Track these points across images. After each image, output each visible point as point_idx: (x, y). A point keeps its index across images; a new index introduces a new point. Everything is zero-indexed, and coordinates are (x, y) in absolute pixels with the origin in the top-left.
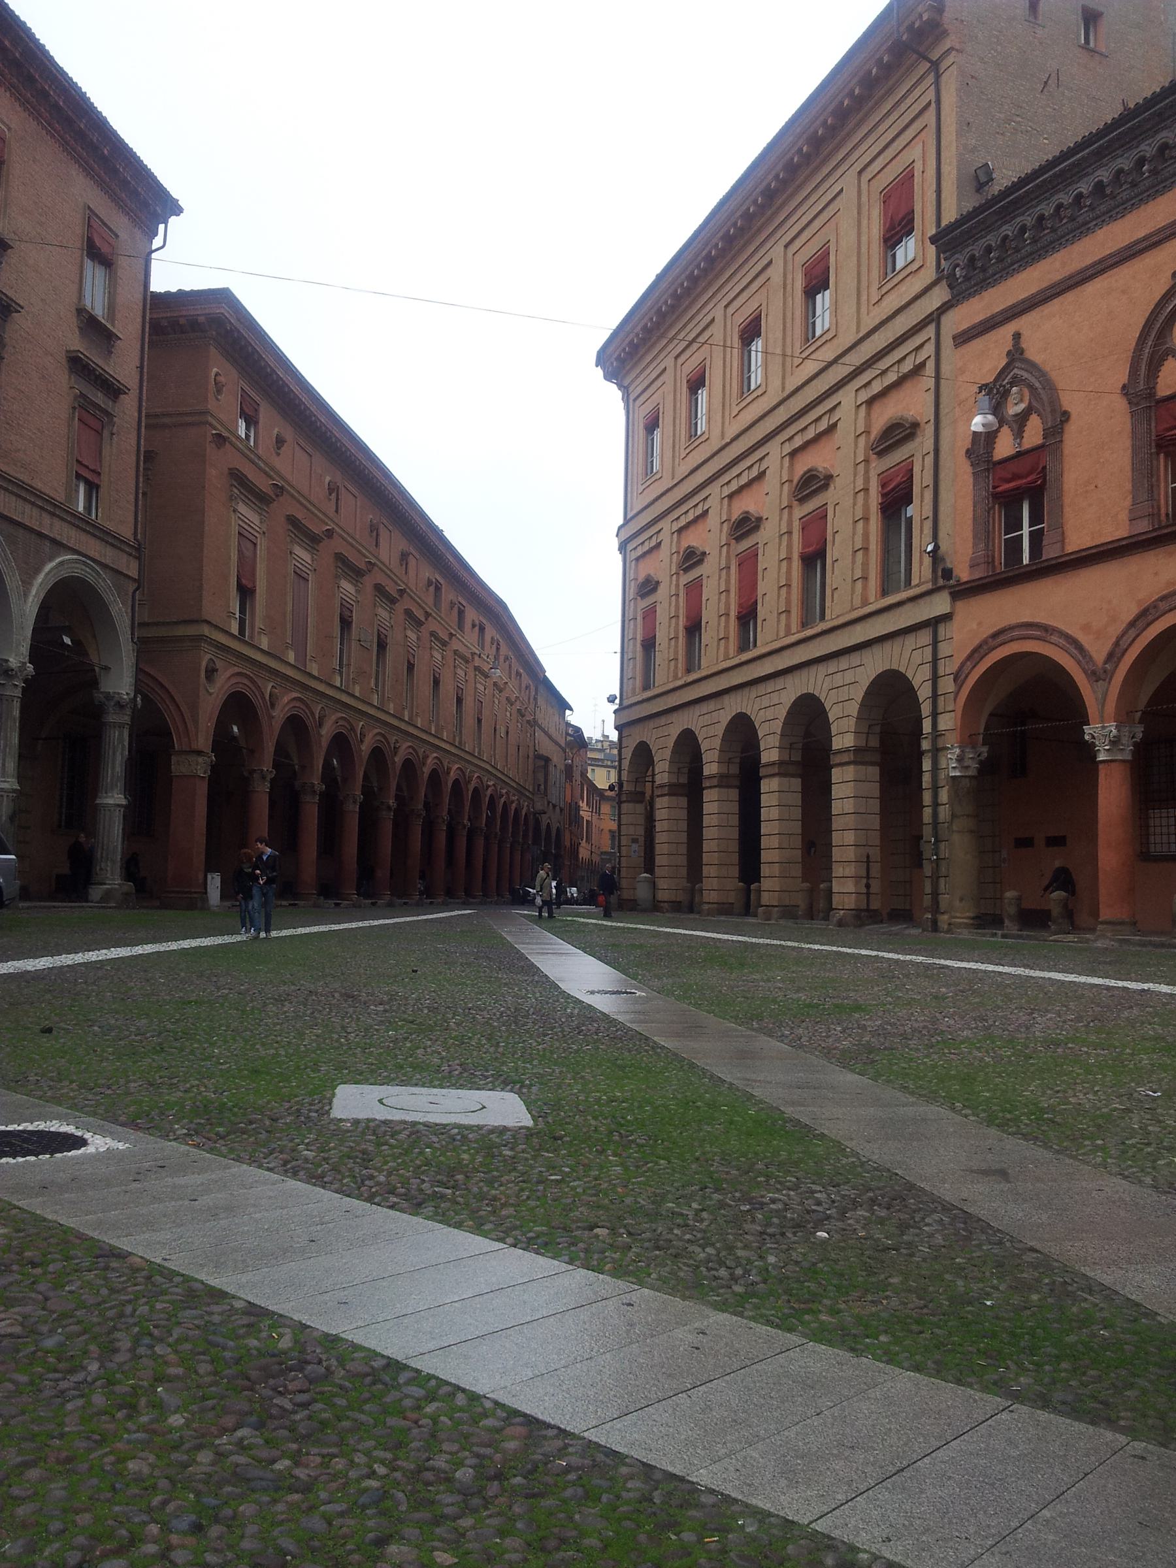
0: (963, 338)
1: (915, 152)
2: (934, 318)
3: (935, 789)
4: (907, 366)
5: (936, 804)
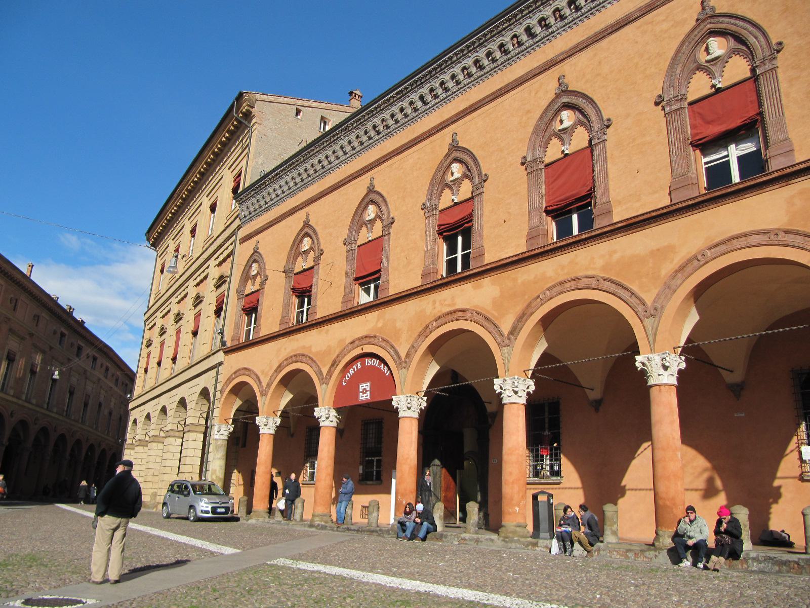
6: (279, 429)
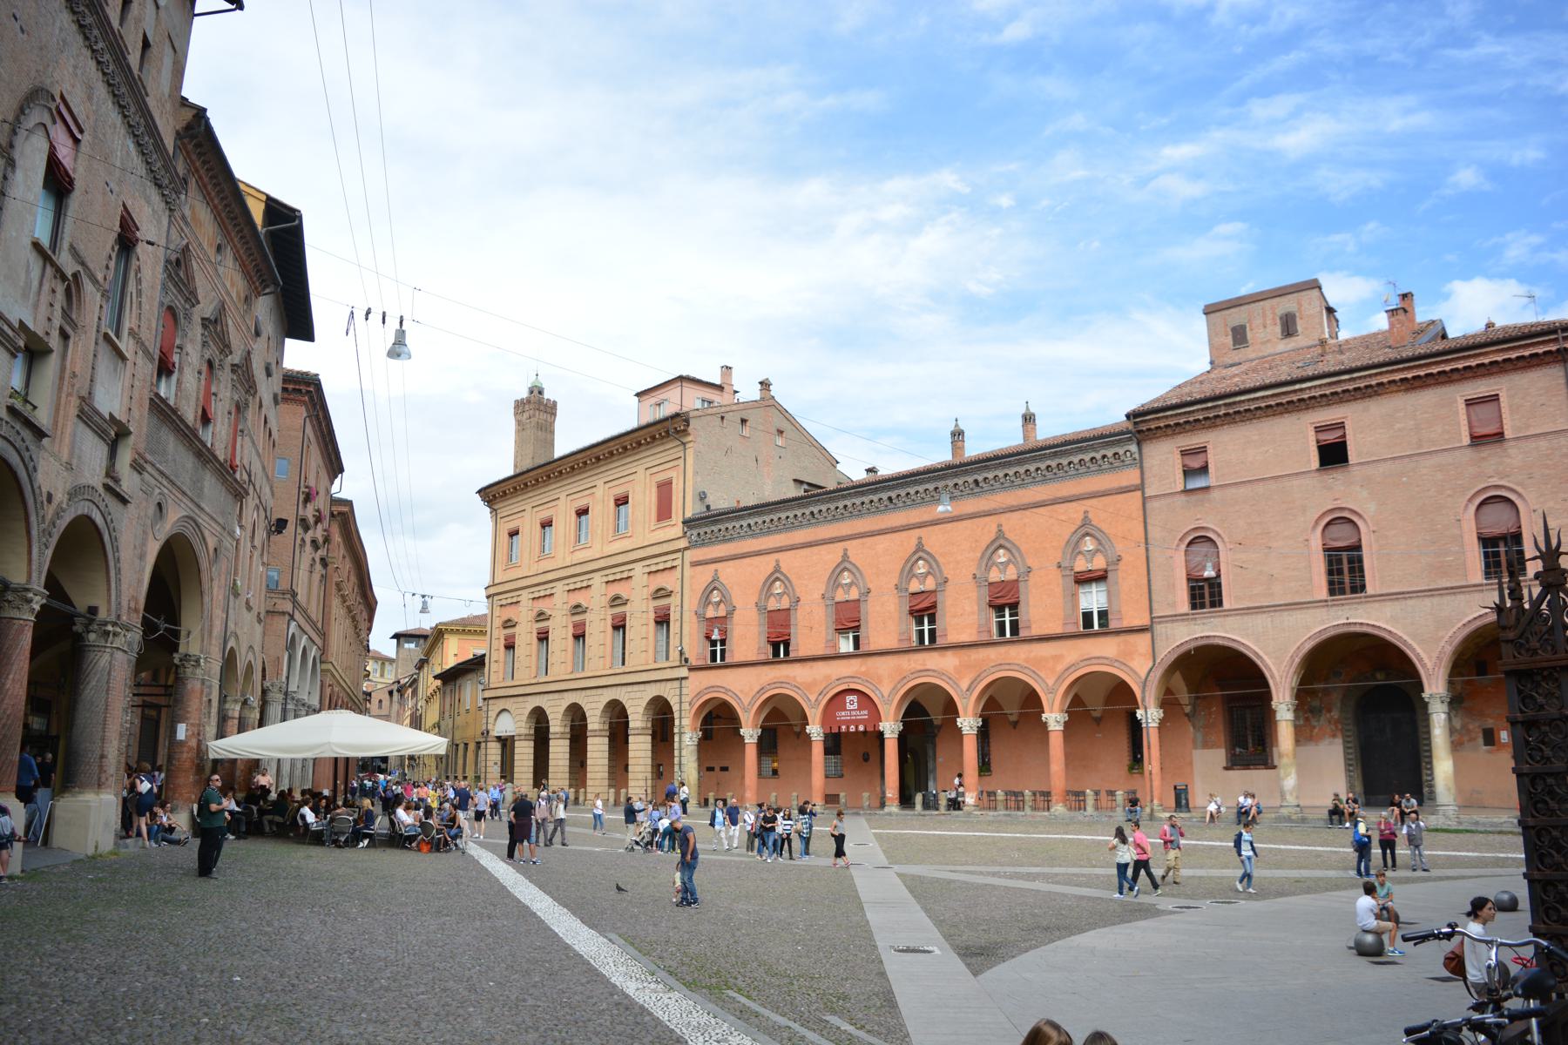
0: (695, 564)
1: (673, 474)
4: (669, 565)
6: (760, 738)
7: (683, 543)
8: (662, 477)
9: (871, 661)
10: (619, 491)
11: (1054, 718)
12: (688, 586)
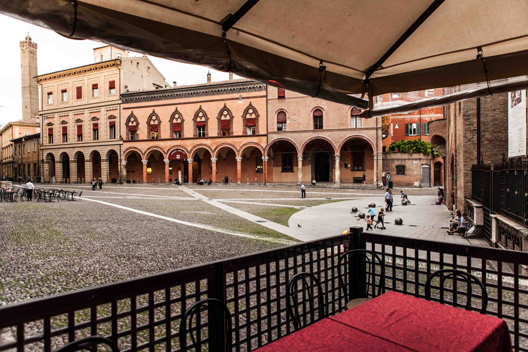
0: (124, 109)
2: (120, 104)
3: (121, 166)
5: (121, 168)
6: (148, 163)
7: (120, 102)
8: (111, 80)
9: (185, 141)
10: (95, 83)
11: (239, 159)
12: (122, 116)
